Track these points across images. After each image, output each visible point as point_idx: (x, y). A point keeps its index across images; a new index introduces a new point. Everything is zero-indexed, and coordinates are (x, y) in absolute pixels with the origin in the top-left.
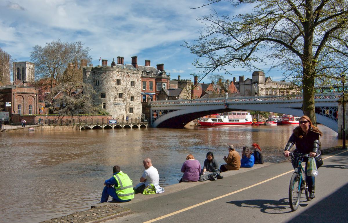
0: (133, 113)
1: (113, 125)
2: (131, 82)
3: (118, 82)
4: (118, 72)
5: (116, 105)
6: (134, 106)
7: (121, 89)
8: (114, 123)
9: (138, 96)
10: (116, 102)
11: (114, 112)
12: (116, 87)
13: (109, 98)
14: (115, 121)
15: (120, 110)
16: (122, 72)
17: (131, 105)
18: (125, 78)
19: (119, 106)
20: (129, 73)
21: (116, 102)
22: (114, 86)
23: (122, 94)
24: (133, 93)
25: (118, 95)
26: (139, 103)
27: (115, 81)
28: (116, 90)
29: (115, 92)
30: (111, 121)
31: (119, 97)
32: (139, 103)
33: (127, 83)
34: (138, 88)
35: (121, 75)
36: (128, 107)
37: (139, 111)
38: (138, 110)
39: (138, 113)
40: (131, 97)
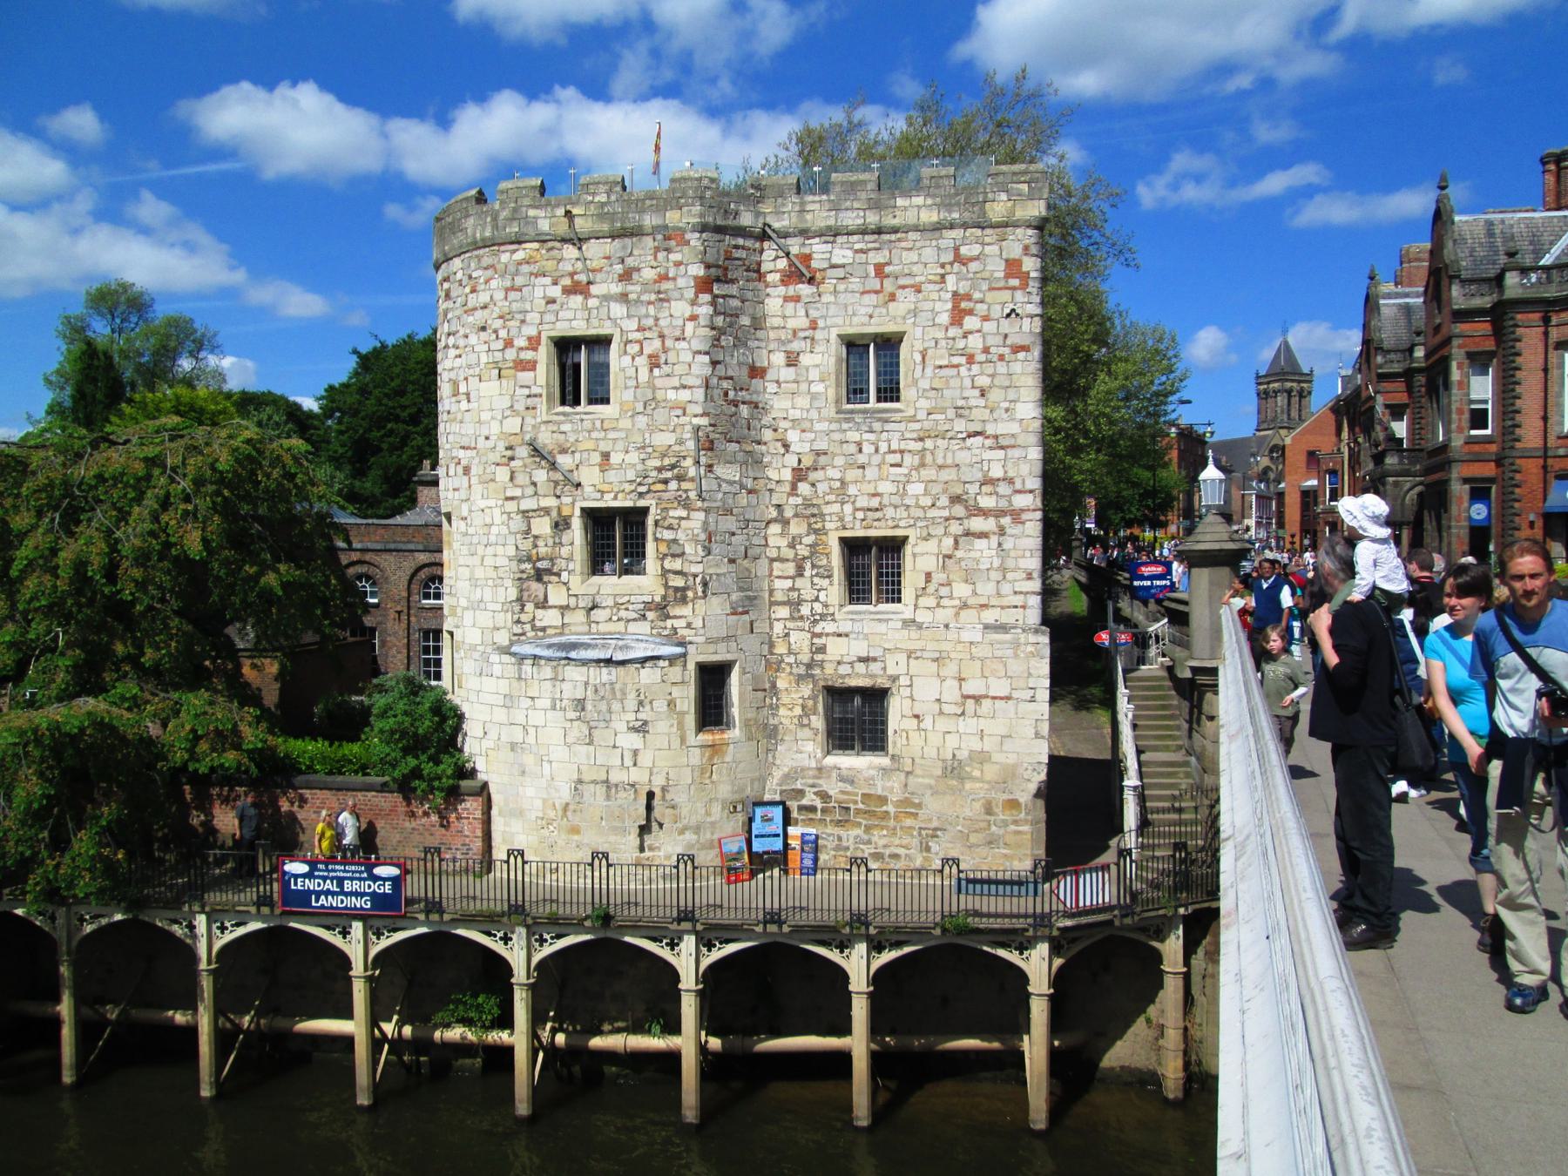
0: (884, 761)
1: (357, 928)
2: (854, 346)
3: (578, 369)
4: (578, 241)
5: (527, 667)
6: (895, 665)
7: (615, 458)
8: (364, 903)
9: (977, 524)
10: (549, 618)
11: (513, 746)
12: (546, 439)
13: (474, 582)
14: (365, 886)
15: (579, 730)
16: (636, 233)
17: (860, 649)
18: (681, 308)
19: (574, 673)
20: (804, 233)
21: (549, 618)
22: (513, 425)
23: (634, 519)
24: (886, 487)
25: (577, 532)
26: (1002, 628)
27: (531, 366)
28: (541, 476)
29: (528, 504)
30: (311, 885)
31: (597, 563)
32: (1002, 628)
33: (757, 372)
34: (960, 426)
35: (626, 276)
36: (800, 679)
37: (995, 727)
38: (969, 725)
39: (982, 758)
40: (854, 548)
